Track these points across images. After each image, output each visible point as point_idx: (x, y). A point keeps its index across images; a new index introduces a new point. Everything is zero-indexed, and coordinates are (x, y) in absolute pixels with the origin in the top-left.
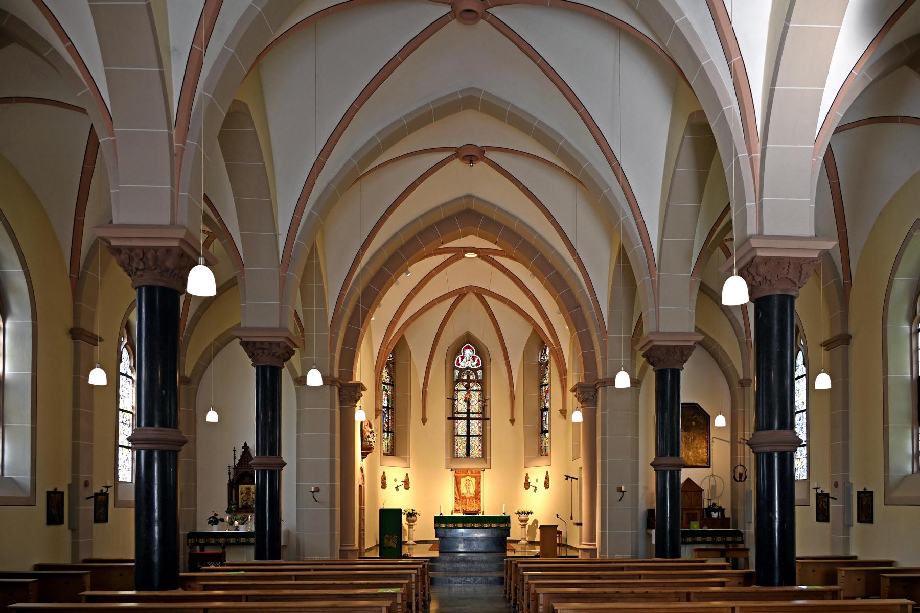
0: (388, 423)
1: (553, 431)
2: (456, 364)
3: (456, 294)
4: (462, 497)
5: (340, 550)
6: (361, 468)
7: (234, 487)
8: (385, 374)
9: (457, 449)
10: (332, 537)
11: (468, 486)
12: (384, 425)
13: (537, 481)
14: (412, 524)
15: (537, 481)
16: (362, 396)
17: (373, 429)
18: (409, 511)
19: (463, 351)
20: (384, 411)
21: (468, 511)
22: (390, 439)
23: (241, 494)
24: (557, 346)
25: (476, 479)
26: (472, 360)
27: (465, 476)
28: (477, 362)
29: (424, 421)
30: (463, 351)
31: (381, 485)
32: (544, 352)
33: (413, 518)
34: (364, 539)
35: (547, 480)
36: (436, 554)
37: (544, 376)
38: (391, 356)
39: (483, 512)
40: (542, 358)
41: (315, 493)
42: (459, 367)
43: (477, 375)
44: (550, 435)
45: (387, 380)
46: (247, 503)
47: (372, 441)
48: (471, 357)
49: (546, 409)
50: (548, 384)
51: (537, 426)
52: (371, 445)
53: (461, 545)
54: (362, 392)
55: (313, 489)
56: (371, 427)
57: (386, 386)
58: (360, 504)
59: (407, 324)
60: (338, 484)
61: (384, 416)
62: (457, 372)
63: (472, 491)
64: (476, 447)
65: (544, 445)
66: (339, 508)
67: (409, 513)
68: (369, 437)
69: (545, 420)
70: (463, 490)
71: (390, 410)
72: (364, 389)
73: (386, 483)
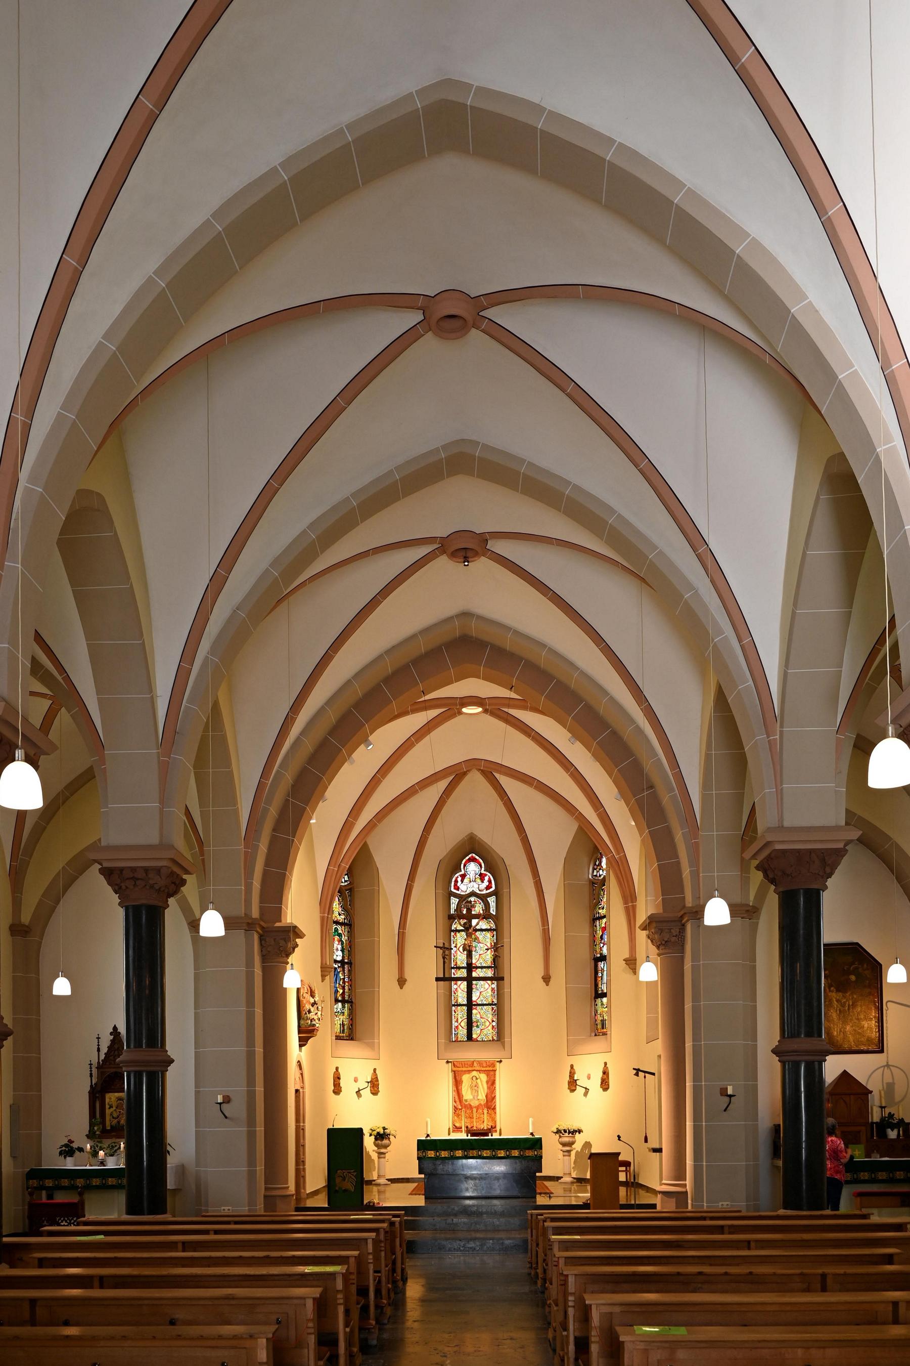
0: (343, 988)
1: (613, 995)
2: (452, 887)
3: (450, 774)
4: (466, 1106)
7: (98, 1097)
8: (336, 907)
9: (457, 1027)
11: (474, 1088)
12: (337, 992)
13: (589, 1078)
14: (383, 1150)
15: (589, 1078)
16: (297, 945)
17: (317, 999)
18: (378, 1130)
19: (465, 866)
20: (335, 969)
21: (475, 1128)
22: (346, 1013)
23: (109, 1108)
24: (618, 853)
25: (487, 1076)
26: (479, 881)
27: (469, 1072)
28: (487, 884)
29: (402, 982)
30: (465, 866)
31: (333, 1088)
32: (597, 863)
33: (385, 1142)
35: (605, 1076)
37: (598, 903)
38: (346, 878)
39: (500, 1130)
40: (595, 874)
43: (487, 905)
44: (609, 1001)
45: (341, 918)
46: (119, 1122)
47: (316, 1017)
48: (477, 876)
49: (603, 958)
50: (604, 917)
51: (588, 986)
52: (314, 1025)
54: (298, 940)
56: (313, 996)
57: (339, 927)
59: (371, 826)
61: (337, 975)
62: (454, 901)
63: (482, 1096)
64: (487, 1023)
65: (599, 1018)
67: (378, 1133)
68: (309, 1012)
69: (602, 977)
70: (467, 1095)
71: (346, 966)
72: (300, 935)
73: (341, 1085)
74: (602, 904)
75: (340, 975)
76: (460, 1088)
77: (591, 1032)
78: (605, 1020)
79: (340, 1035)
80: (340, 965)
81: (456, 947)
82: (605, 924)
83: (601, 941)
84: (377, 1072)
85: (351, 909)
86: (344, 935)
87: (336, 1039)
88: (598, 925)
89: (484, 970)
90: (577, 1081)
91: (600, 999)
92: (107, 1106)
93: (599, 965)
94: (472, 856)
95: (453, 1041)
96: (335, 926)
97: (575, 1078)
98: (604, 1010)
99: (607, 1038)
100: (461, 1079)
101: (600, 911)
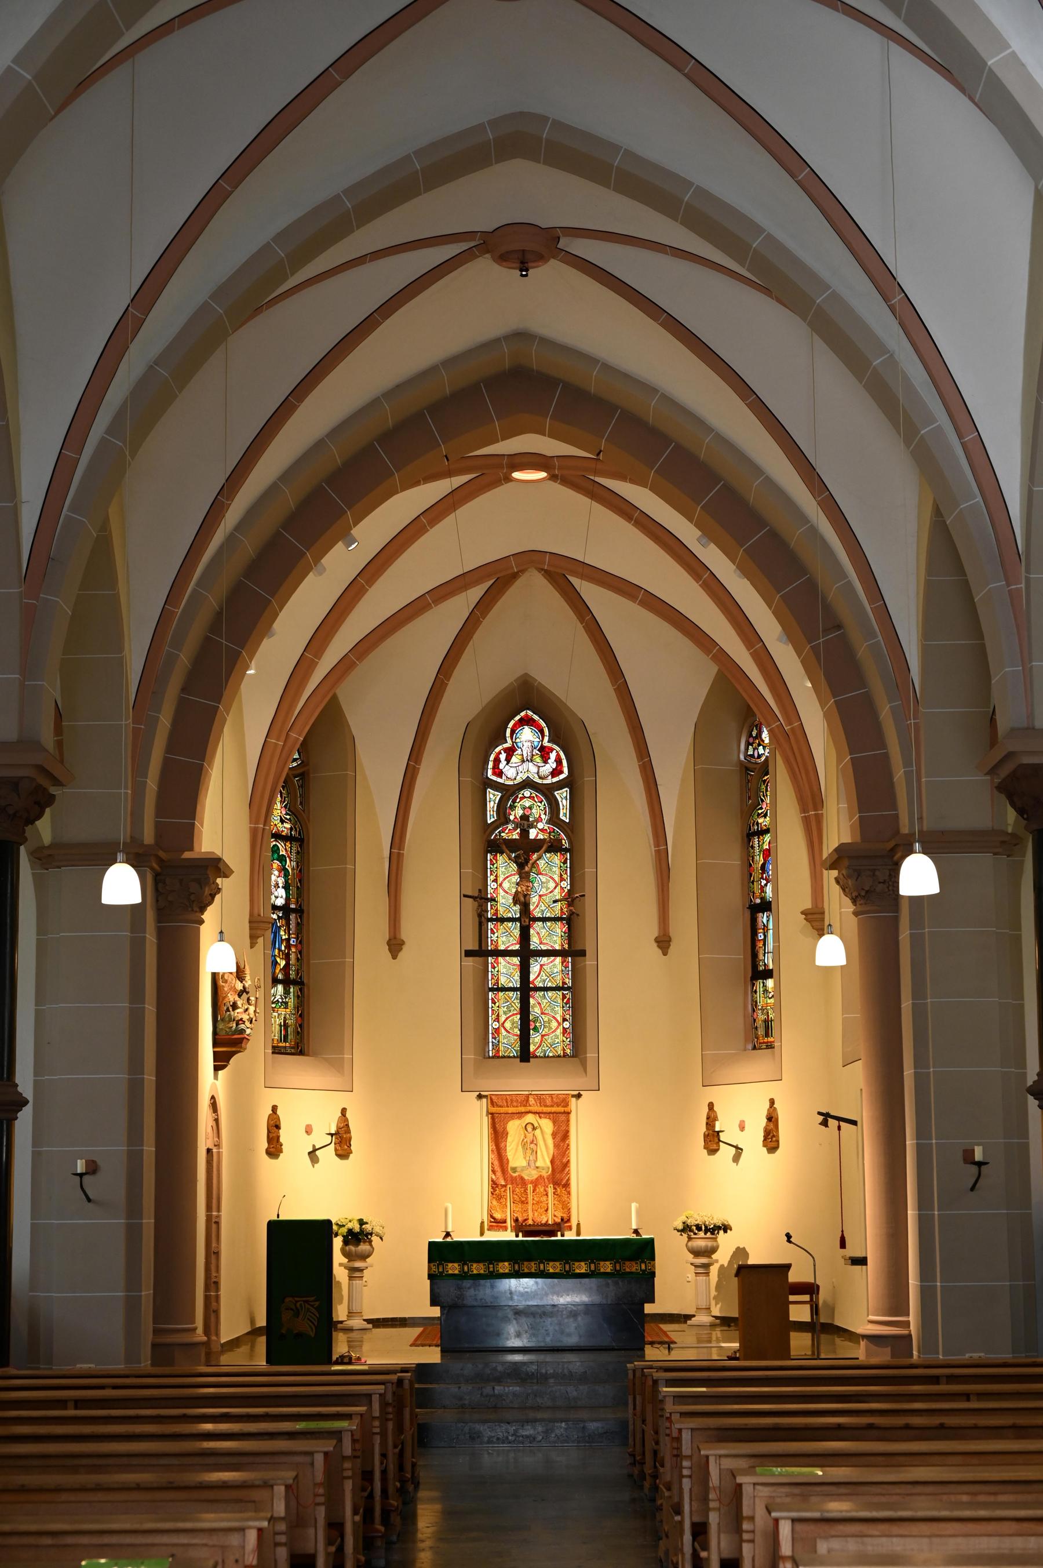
0: (287, 957)
1: (785, 973)
2: (490, 772)
4: (514, 1181)
5: (154, 1346)
6: (213, 1097)
8: (279, 810)
9: (497, 1031)
10: (132, 1305)
11: (530, 1146)
12: (275, 963)
13: (742, 1128)
14: (358, 1264)
15: (742, 1128)
18: (350, 1225)
21: (530, 1222)
22: (291, 1004)
25: (554, 1123)
26: (538, 759)
27: (521, 1115)
28: (554, 766)
29: (395, 946)
31: (266, 1145)
32: (754, 733)
33: (363, 1247)
34: (217, 1312)
35: (771, 1126)
36: (432, 1356)
37: (757, 805)
38: (296, 756)
39: (578, 1225)
40: (750, 752)
41: (86, 1178)
42: (499, 780)
44: (778, 986)
45: (285, 828)
48: (536, 751)
49: (766, 906)
50: (767, 831)
51: (739, 956)
53: (511, 1329)
55: (80, 1166)
57: (281, 845)
58: (209, 1208)
59: (345, 666)
60: (149, 1148)
61: (276, 933)
62: (493, 797)
63: (544, 1160)
64: (554, 1024)
65: (761, 1017)
66: (153, 1221)
67: (350, 1231)
69: (764, 940)
70: (516, 1158)
71: (292, 917)
73: (281, 1140)
74: (764, 806)
75: (282, 933)
76: (502, 1145)
77: (746, 1041)
78: (771, 1021)
79: (281, 1045)
80: (281, 915)
81: (495, 880)
82: (769, 843)
83: (762, 874)
84: (348, 1115)
85: (304, 811)
86: (290, 858)
87: (273, 1053)
88: (756, 845)
89: (549, 924)
90: (720, 1134)
91: (761, 981)
93: (759, 920)
94: (527, 715)
95: (489, 1057)
96: (274, 843)
97: (717, 1129)
98: (769, 1001)
99: (773, 1054)
100: (505, 1129)
101: (760, 820)
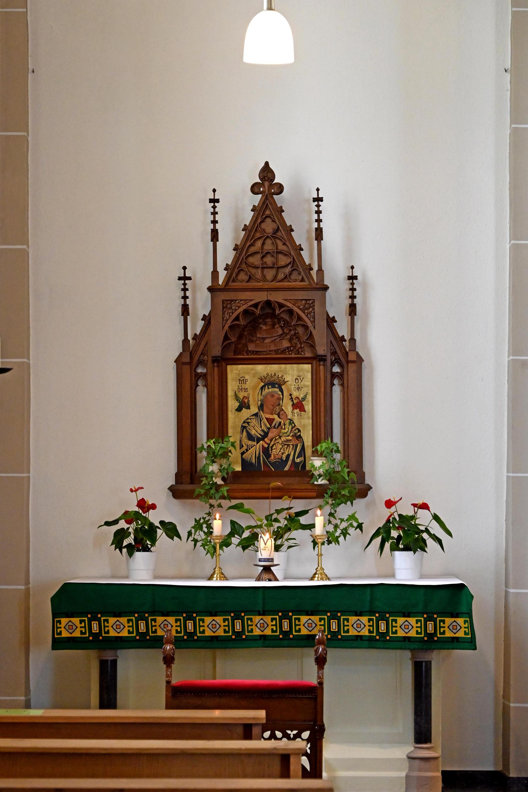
7: (204, 376)
23: (239, 409)
46: (266, 451)
92: (232, 404)
